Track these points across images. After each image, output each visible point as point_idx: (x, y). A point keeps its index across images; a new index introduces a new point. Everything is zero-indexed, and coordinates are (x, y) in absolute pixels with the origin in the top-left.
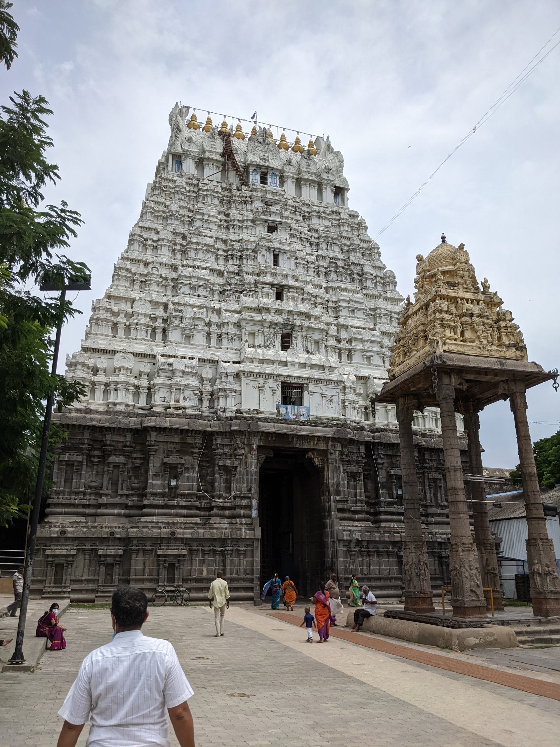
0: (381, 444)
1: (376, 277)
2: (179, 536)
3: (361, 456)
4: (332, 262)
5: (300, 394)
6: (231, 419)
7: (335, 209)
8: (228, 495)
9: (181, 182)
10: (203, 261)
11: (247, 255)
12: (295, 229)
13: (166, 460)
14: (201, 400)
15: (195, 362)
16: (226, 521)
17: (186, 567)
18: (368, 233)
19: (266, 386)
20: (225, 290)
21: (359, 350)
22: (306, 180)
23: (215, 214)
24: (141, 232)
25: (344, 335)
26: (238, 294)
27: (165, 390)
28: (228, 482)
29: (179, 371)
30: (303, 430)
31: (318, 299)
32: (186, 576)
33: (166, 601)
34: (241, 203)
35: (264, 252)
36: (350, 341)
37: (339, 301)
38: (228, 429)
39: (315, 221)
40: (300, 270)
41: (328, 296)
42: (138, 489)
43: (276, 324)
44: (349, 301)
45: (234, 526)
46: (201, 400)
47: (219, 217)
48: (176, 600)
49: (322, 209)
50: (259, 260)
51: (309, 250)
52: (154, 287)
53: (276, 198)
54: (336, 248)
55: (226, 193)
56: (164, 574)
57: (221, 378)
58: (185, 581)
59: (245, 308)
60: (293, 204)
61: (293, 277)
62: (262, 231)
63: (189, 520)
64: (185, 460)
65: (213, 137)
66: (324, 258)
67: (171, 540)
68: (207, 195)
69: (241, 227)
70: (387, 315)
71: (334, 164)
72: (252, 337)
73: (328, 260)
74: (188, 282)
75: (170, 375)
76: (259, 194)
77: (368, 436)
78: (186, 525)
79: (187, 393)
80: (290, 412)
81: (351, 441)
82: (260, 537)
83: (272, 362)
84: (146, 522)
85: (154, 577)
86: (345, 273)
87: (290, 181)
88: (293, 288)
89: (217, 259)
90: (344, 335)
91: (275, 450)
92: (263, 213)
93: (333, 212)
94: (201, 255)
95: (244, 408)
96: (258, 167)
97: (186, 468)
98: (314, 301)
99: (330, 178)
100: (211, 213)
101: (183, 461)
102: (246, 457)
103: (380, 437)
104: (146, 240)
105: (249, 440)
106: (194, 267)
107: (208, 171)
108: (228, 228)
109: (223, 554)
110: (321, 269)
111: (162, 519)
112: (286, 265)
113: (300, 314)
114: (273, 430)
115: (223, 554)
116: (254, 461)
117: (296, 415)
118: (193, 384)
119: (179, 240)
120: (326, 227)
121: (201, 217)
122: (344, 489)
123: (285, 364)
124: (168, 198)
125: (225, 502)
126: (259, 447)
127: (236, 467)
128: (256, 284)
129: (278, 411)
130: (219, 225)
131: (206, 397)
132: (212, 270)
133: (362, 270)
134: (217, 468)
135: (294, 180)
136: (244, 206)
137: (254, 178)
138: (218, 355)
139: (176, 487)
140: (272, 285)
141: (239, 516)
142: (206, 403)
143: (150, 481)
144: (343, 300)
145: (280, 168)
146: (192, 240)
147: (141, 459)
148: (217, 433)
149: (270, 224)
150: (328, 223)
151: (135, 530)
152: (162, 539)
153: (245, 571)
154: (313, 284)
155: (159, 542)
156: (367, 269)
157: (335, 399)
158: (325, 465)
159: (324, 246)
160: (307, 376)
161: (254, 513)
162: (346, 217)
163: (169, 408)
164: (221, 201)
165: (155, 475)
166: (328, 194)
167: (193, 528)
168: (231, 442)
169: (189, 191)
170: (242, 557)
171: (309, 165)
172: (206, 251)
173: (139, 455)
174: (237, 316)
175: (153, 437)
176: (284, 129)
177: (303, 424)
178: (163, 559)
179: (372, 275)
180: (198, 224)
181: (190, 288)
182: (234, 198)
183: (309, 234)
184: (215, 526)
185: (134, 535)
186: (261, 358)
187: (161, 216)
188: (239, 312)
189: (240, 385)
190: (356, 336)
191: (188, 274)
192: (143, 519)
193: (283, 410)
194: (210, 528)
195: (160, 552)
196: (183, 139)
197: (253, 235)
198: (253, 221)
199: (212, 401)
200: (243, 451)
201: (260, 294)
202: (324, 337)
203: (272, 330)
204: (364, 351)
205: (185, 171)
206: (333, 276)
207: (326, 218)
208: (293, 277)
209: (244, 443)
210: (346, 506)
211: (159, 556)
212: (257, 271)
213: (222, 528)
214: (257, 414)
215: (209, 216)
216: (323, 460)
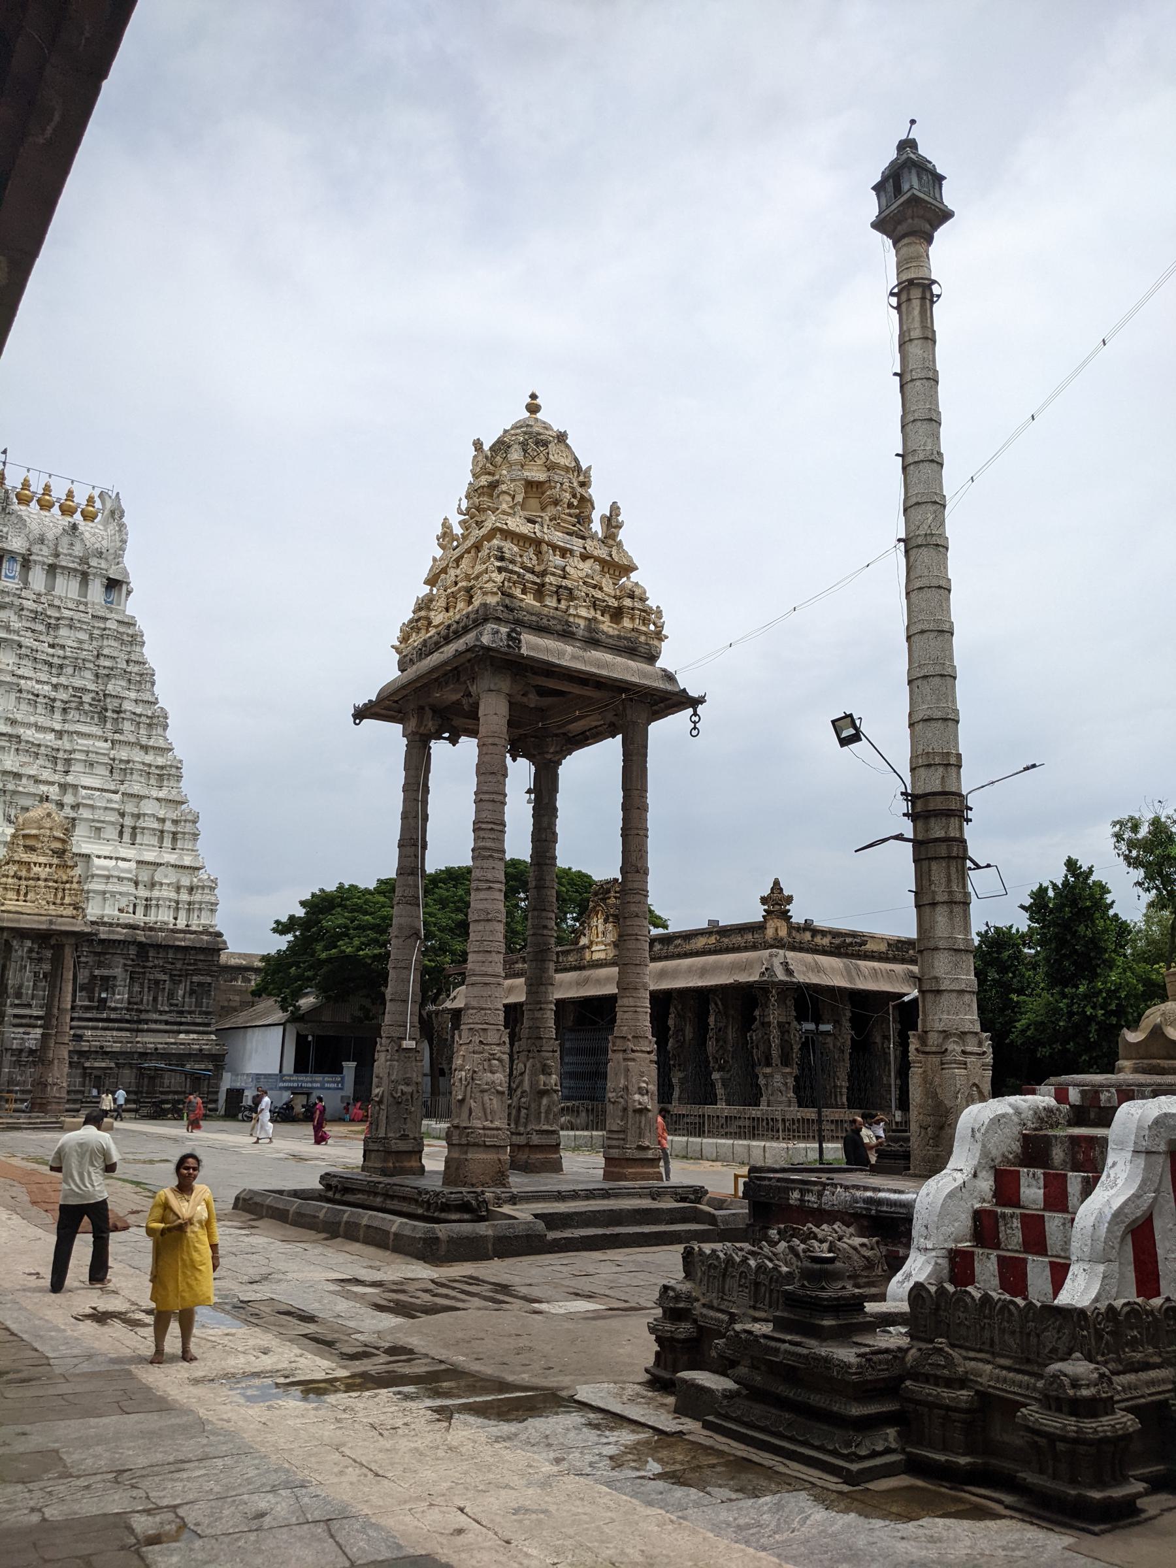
1: (140, 715)
7: (100, 614)
12: (27, 647)
18: (144, 650)
21: (86, 820)
25: (69, 799)
31: (43, 748)
36: (76, 807)
37: (75, 751)
39: (63, 632)
40: (24, 707)
41: (60, 742)
44: (87, 753)
51: (44, 677)
53: (7, 600)
60: (34, 606)
90: (69, 799)
98: (34, 750)
99: (104, 565)
120: (81, 642)
150: (84, 636)
156: (128, 706)
159: (70, 670)
171: (72, 544)
179: (134, 713)
183: (51, 651)
204: (93, 821)
206: (73, 715)
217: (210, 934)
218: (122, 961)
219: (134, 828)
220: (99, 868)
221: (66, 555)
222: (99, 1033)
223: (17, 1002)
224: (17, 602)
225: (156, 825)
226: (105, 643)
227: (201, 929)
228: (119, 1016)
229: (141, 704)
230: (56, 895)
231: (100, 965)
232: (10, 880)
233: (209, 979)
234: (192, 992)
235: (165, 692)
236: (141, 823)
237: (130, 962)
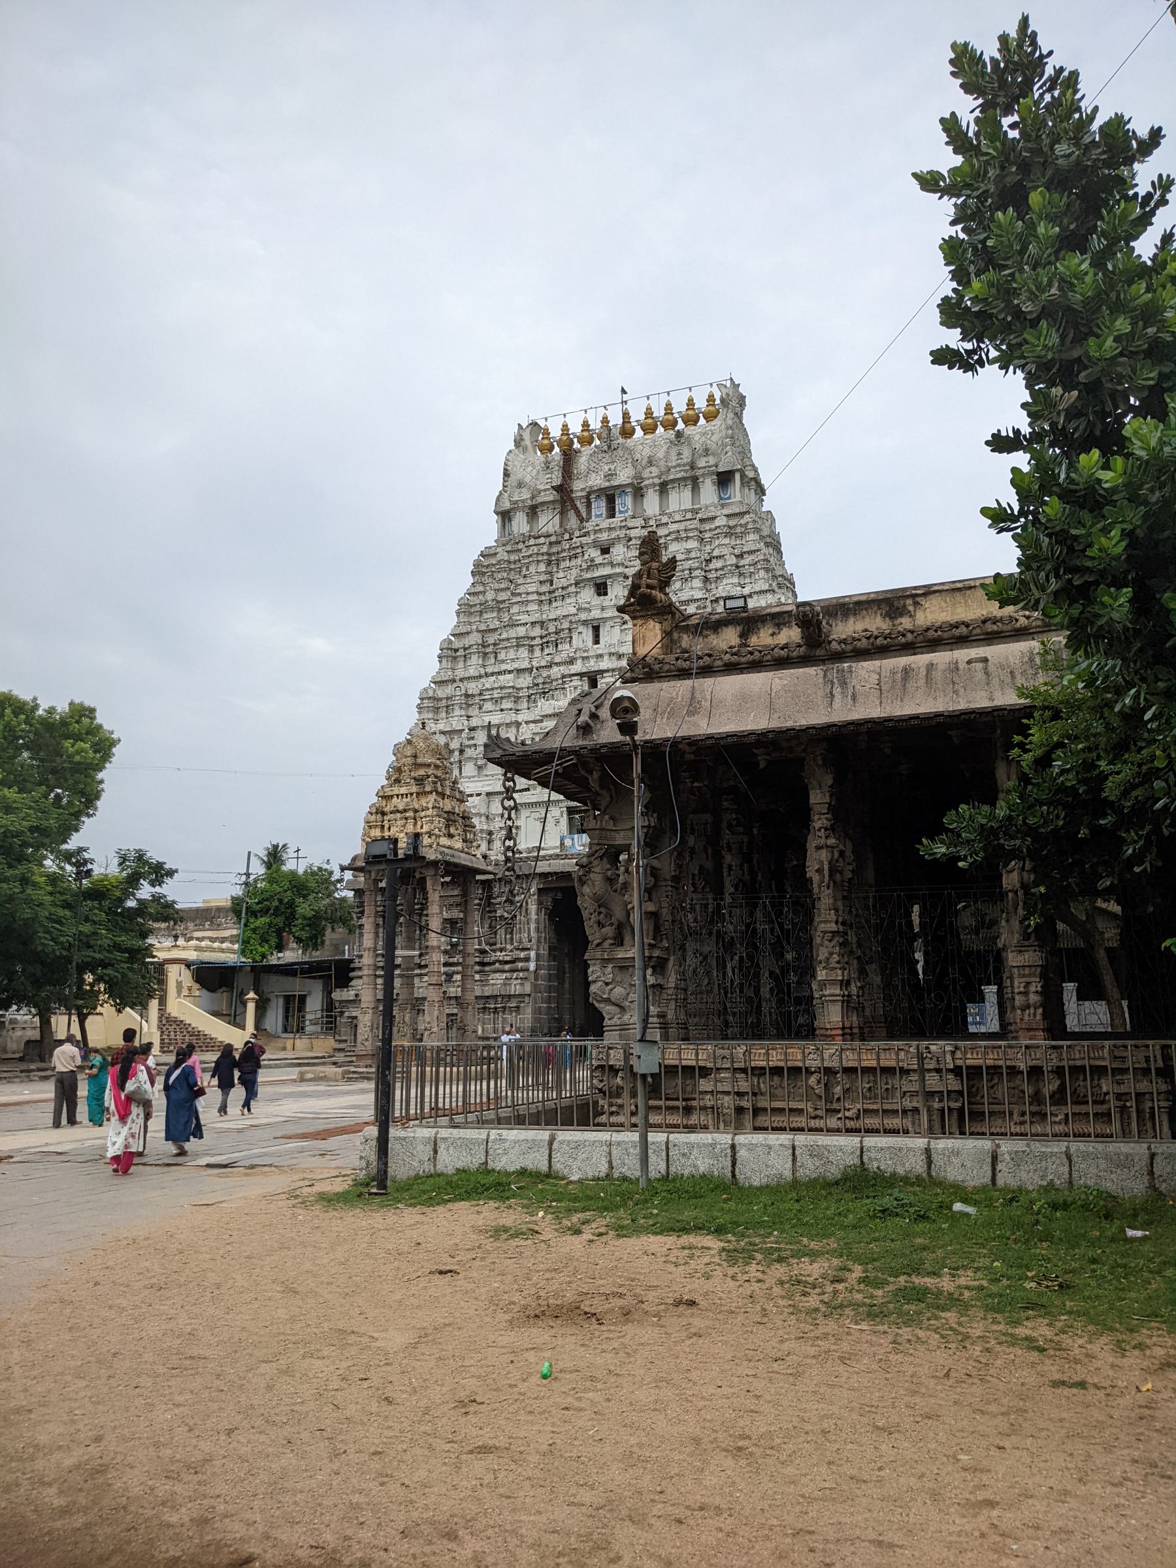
10: (513, 660)
16: (504, 976)
23: (534, 589)
35: (581, 629)
52: (457, 712)
62: (587, 595)
88: (607, 671)
92: (588, 568)
94: (512, 654)
96: (601, 492)
99: (712, 460)
100: (530, 590)
104: (456, 650)
107: (543, 519)
114: (548, 870)
116: (533, 908)
120: (689, 551)
126: (539, 889)
128: (564, 677)
137: (599, 507)
161: (532, 966)
164: (549, 563)
172: (517, 646)
180: (515, 609)
193: (568, 842)
205: (516, 532)
208: (611, 654)
215: (528, 594)
224: (622, 533)
226: (717, 542)
229: (755, 597)
230: (415, 824)
232: (373, 818)
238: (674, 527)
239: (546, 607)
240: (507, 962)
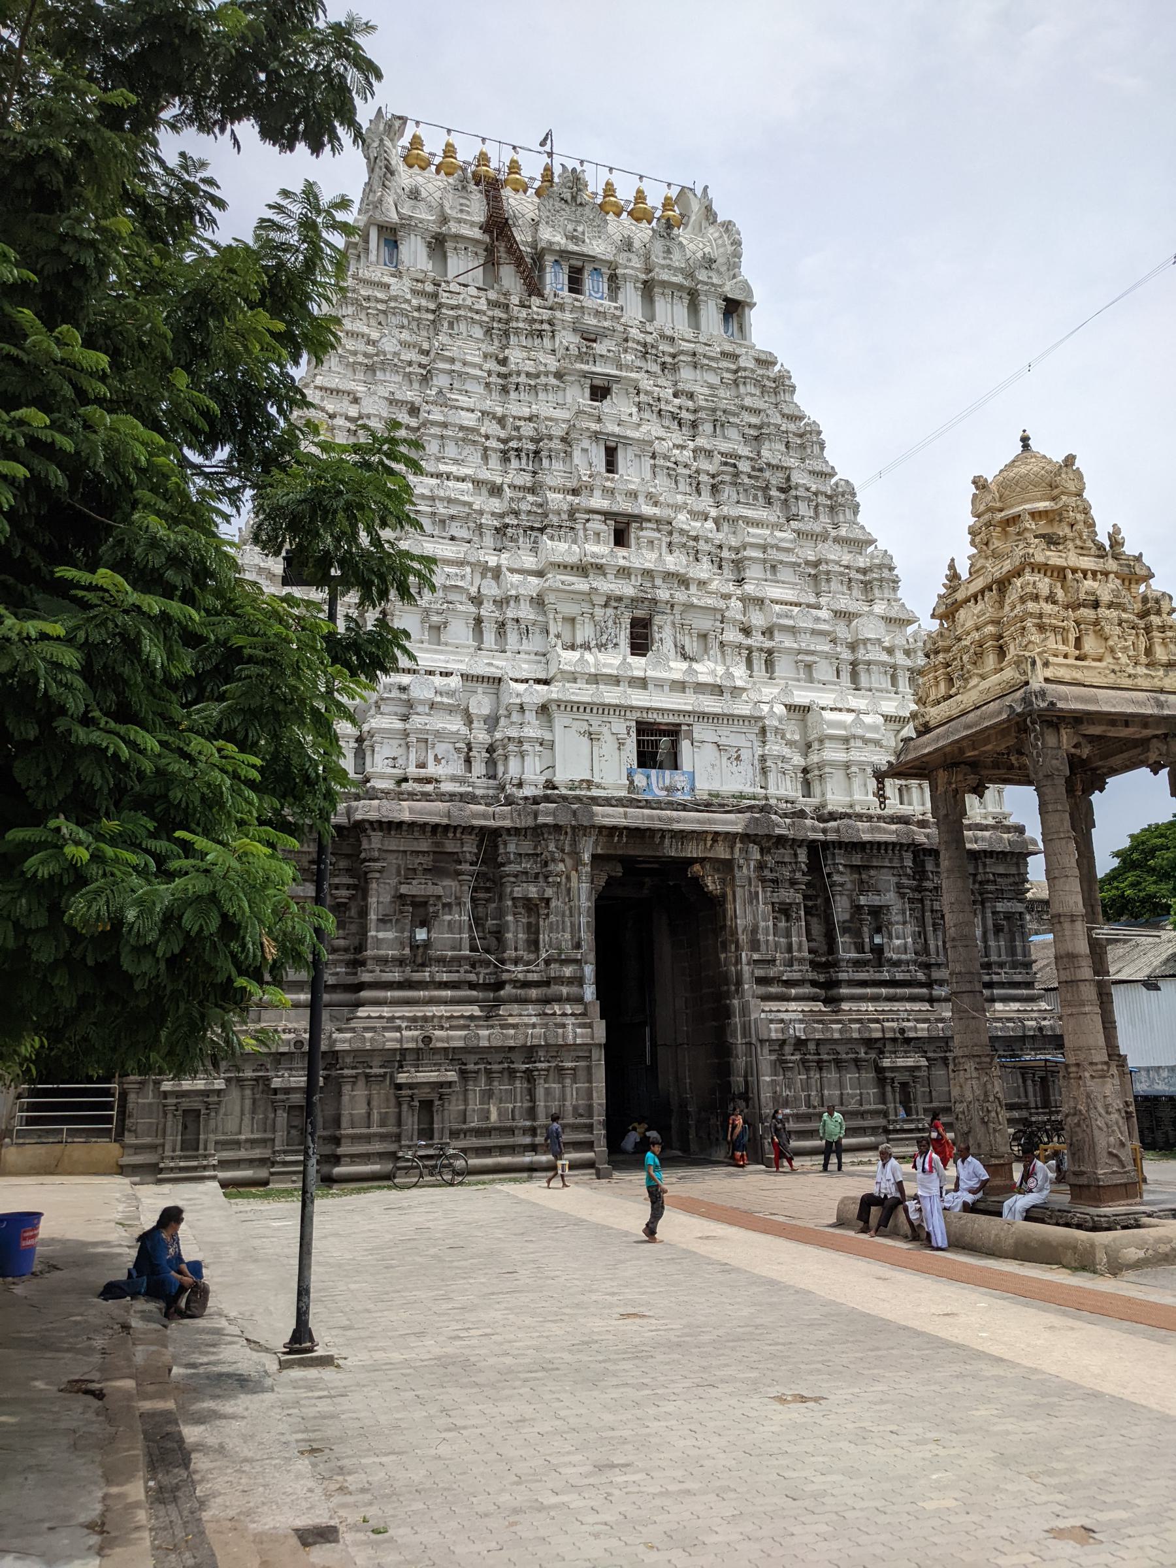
0: (840, 844)
1: (816, 494)
2: (439, 1045)
3: (800, 870)
4: (726, 464)
5: (675, 745)
6: (536, 801)
7: (728, 348)
8: (532, 956)
9: (400, 287)
10: (456, 462)
11: (550, 450)
12: (647, 393)
13: (404, 889)
14: (468, 761)
15: (454, 682)
16: (531, 1009)
17: (454, 1107)
18: (797, 398)
19: (605, 730)
20: (506, 526)
21: (789, 651)
22: (664, 284)
23: (478, 360)
24: (322, 399)
25: (757, 619)
26: (534, 534)
27: (395, 743)
28: (533, 931)
29: (422, 702)
30: (685, 821)
31: (702, 542)
32: (456, 1126)
33: (421, 1176)
34: (531, 334)
35: (586, 444)
36: (768, 632)
37: (745, 547)
38: (530, 822)
39: (686, 373)
41: (720, 536)
42: (346, 950)
43: (619, 599)
44: (764, 548)
45: (551, 1021)
46: (468, 761)
47: (487, 366)
48: (440, 1173)
49: (701, 349)
50: (576, 461)
53: (606, 324)
54: (733, 433)
55: (498, 313)
56: (411, 1122)
57: (509, 716)
58: (454, 1134)
59: (552, 564)
61: (649, 496)
62: (578, 396)
63: (458, 1010)
64: (444, 887)
65: (464, 188)
66: (709, 454)
67: (424, 1052)
68: (457, 318)
69: (533, 389)
70: (842, 574)
71: (721, 250)
72: (568, 626)
73: (718, 458)
74: (429, 509)
75: (403, 710)
76: (568, 316)
77: (814, 829)
78: (452, 1021)
79: (442, 748)
80: (655, 783)
81: (781, 840)
82: (603, 1041)
83: (616, 680)
84: (369, 1017)
85: (393, 1129)
86: (754, 487)
87: (630, 286)
89: (485, 458)
91: (628, 862)
92: (581, 357)
93: (723, 353)
94: (451, 450)
95: (560, 777)
96: (564, 254)
97: (444, 905)
98: (692, 546)
99: (715, 281)
100: (469, 358)
101: (439, 891)
102: (568, 878)
103: (838, 830)
105: (574, 843)
106: (438, 476)
108: (505, 390)
109: (530, 1077)
110: (704, 478)
111: (400, 1011)
112: (633, 472)
113: (669, 576)
114: (623, 822)
115: (530, 1077)
116: (585, 886)
117: (667, 789)
118: (454, 728)
119: (403, 417)
121: (447, 366)
122: (767, 937)
123: (643, 683)
124: (373, 322)
125: (528, 971)
126: (595, 857)
127: (548, 900)
129: (632, 782)
130: (487, 385)
131: (480, 757)
132: (477, 483)
133: (788, 479)
134: (510, 903)
135: (639, 285)
136: (537, 341)
137: (555, 280)
138: (499, 665)
139: (427, 944)
140: (607, 515)
141: (559, 1000)
142: (479, 768)
143: (373, 933)
144: (753, 545)
145: (610, 257)
146: (431, 417)
147: (348, 887)
148: (508, 830)
149: (597, 382)
150: (714, 379)
151: (348, 1035)
152: (404, 1052)
153: (575, 1108)
154: (689, 511)
155: (400, 1057)
156: (798, 478)
157: (745, 754)
158: (728, 890)
159: (707, 428)
160: (689, 708)
161: (589, 992)
162: (751, 364)
163: (406, 780)
164: (489, 331)
165: (383, 921)
166: (711, 313)
167: (466, 1027)
168: (535, 848)
169: (419, 309)
170: (568, 1081)
171: (668, 251)
172: (463, 440)
173: (346, 880)
174: (534, 580)
175: (375, 842)
176: (611, 169)
177: (685, 808)
178: (409, 1092)
179: (808, 489)
180: (441, 381)
181: (434, 523)
182: (514, 324)
183: (677, 401)
184: (511, 1020)
185: (346, 1047)
186: (593, 670)
187: (361, 364)
188: (540, 574)
189: (551, 728)
190: (782, 621)
191: (427, 492)
192: (362, 1012)
194: (503, 1027)
195: (402, 1078)
196: (400, 191)
197: (561, 407)
198: (559, 375)
199: (491, 763)
200: (561, 867)
201: (581, 533)
202: (718, 624)
203: (610, 611)
205: (407, 263)
206: (728, 492)
207: (710, 368)
208: (649, 496)
209: (563, 851)
210: (772, 972)
211: (399, 1087)
212: (574, 484)
213: (526, 1025)
214: (589, 789)
215: (465, 364)
216: (723, 881)
217: (1008, 829)
218: (894, 880)
219: (854, 664)
220: (832, 724)
221: (663, 267)
222: (887, 1006)
223: (756, 956)
225: (885, 657)
227: (991, 821)
228: (907, 976)
231: (863, 887)
233: (1020, 907)
234: (998, 930)
235: (844, 456)
236: (861, 654)
237: (905, 881)
238: (686, 346)
239: (495, 395)
240: (526, 984)
